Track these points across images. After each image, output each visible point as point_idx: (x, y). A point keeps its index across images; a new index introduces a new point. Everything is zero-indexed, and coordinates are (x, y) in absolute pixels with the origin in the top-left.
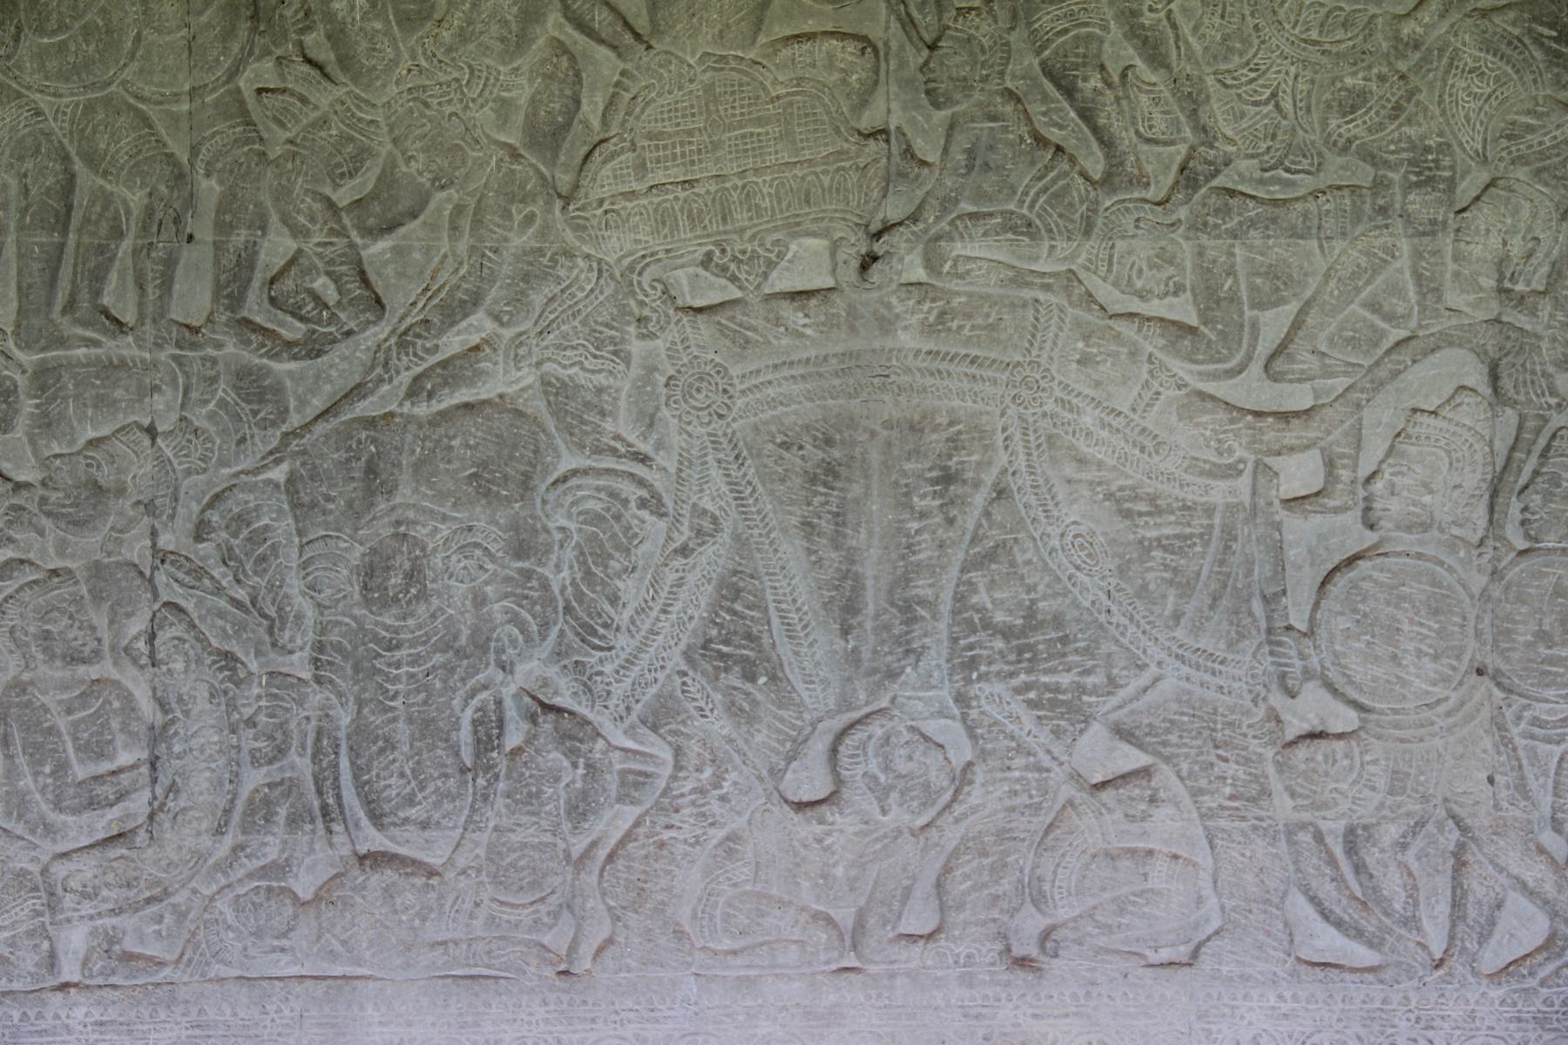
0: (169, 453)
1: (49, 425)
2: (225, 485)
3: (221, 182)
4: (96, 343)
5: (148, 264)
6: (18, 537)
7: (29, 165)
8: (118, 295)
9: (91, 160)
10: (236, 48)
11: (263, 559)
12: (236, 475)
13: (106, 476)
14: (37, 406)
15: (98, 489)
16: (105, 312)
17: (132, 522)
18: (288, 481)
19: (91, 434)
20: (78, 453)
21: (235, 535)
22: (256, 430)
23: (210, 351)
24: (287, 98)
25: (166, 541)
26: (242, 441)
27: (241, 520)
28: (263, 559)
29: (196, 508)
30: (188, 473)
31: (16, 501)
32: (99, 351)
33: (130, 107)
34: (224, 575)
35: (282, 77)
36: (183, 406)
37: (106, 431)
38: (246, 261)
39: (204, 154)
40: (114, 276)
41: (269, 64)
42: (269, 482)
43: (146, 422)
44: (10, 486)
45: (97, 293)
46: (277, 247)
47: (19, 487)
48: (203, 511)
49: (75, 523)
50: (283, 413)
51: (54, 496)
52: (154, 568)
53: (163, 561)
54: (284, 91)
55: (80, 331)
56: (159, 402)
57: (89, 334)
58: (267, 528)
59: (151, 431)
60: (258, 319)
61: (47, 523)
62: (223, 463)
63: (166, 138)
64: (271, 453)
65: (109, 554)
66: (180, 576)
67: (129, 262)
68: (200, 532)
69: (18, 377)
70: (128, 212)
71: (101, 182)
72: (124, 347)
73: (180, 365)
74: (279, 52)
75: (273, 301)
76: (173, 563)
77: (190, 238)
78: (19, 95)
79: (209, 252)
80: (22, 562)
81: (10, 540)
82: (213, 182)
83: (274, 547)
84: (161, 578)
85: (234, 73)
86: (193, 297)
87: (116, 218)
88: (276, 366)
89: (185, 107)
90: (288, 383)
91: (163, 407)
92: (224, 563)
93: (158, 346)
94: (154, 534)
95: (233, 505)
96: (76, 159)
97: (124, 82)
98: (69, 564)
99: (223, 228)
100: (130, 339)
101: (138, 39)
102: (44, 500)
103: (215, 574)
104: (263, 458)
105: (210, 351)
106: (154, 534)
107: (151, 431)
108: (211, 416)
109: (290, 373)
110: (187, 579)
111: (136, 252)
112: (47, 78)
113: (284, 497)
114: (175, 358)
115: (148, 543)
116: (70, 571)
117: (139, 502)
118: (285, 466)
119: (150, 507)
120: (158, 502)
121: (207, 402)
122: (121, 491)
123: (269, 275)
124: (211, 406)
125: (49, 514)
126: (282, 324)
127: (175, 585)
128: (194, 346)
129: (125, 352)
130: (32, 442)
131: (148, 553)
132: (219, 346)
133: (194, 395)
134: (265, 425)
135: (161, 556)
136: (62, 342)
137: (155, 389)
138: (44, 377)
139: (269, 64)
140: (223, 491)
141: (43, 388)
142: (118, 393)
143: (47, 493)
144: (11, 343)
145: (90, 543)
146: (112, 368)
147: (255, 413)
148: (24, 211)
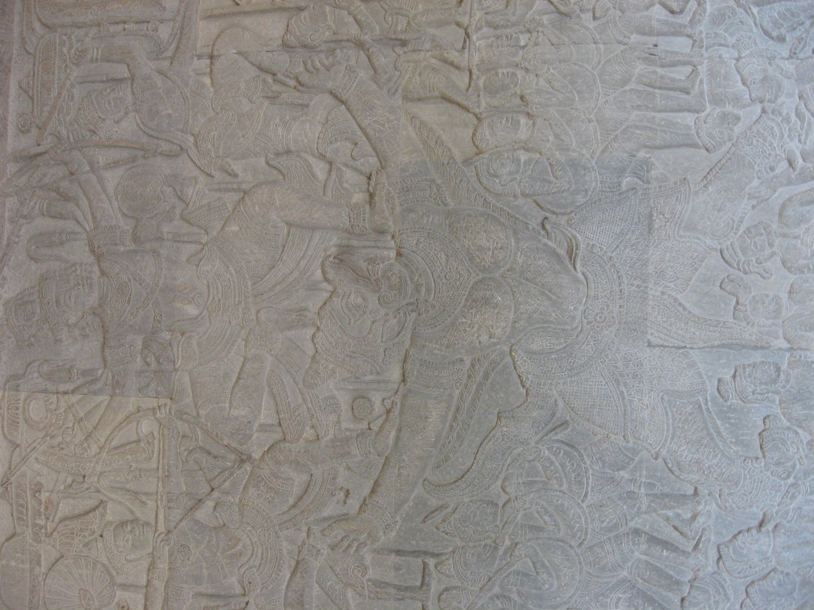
0: (748, 52)
1: (737, 99)
2: (761, 30)
3: (632, 33)
4: (702, 80)
5: (668, 59)
6: (786, 112)
7: (628, 105)
8: (680, 74)
9: (625, 82)
10: (577, 27)
11: (793, 15)
12: (756, 24)
13: (758, 77)
14: (729, 103)
15: (765, 79)
16: (688, 77)
17: (778, 66)
18: (758, 6)
19: (740, 83)
20: (748, 87)
21: (782, 25)
22: (737, 17)
23: (704, 35)
24: (597, 7)
25: (785, 53)
26: (741, 22)
27: (776, 24)
28: (793, 15)
29: (771, 42)
30: (756, 44)
31: (770, 112)
32: (704, 80)
33: (603, 66)
34: (800, 30)
35: (588, 10)
36: (727, 46)
37: (738, 78)
38: (666, 23)
39: (621, 38)
40: (672, 75)
41: (583, 16)
42: (758, 13)
43: (734, 61)
44: (763, 115)
45: (680, 80)
46: (658, 12)
47: (764, 111)
48: (772, 38)
49: (780, 88)
50: (729, 7)
51: (768, 97)
52: (797, 58)
53: (795, 53)
54: (594, 8)
55: (696, 87)
56: (726, 56)
57: (698, 82)
58: (778, 13)
59: (738, 60)
60: (689, 19)
61: (779, 101)
62: (751, 31)
63: (616, 53)
64: (746, 11)
65: (793, 75)
66: (801, 46)
67: (666, 69)
68: (781, 39)
69: (717, 111)
70: (646, 69)
71: (634, 79)
72: (703, 69)
73: (710, 47)
74: (578, 11)
75: (682, 12)
76: (796, 49)
77: (656, 46)
78: (600, 108)
79: (661, 38)
80: (797, 109)
81: (787, 114)
82: (632, 37)
83: (787, 10)
84: (801, 56)
85: (587, 28)
86: (681, 45)
87: (649, 72)
88: (709, 11)
89: (602, 46)
90: (716, 7)
91: (726, 54)
92: (795, 29)
93: (702, 56)
94: (783, 58)
95: (768, 26)
96: (625, 88)
97: (593, 69)
98: (797, 92)
99: (650, 33)
100: (699, 67)
101: (575, 64)
102: (769, 101)
103: (799, 34)
104: (749, 14)
105: (704, 35)
106: (783, 58)
107: (738, 60)
108: (731, 35)
109: (711, 6)
110: (803, 43)
111: (662, 66)
112: (592, 98)
113: (765, 7)
114: (707, 50)
115: (786, 62)
116: (800, 92)
117: (770, 64)
118: (752, 7)
119: (771, 59)
120: (769, 55)
121: (725, 37)
122: (765, 70)
123: (670, 15)
124: (727, 35)
125: (776, 99)
126: (690, 10)
127: (805, 50)
128: (701, 41)
129: (705, 69)
130: (744, 107)
131: (791, 61)
132: (701, 32)
133: (722, 42)
134: (734, 13)
135: (793, 55)
136: (702, 93)
137: (720, 56)
138: (717, 100)
139: (583, 16)
140: (763, 30)
141: (722, 100)
142: (723, 71)
143: (767, 99)
144: (703, 114)
145: (787, 84)
146: (712, 74)
147: (729, 17)
148: (647, 108)
